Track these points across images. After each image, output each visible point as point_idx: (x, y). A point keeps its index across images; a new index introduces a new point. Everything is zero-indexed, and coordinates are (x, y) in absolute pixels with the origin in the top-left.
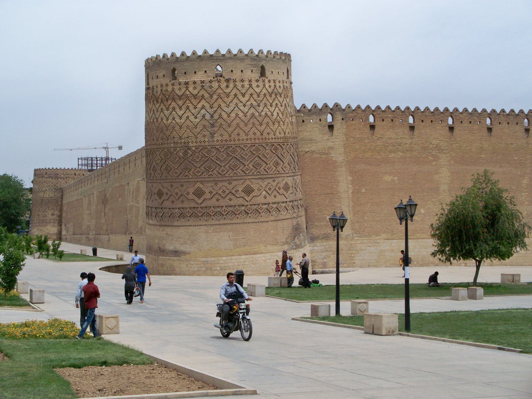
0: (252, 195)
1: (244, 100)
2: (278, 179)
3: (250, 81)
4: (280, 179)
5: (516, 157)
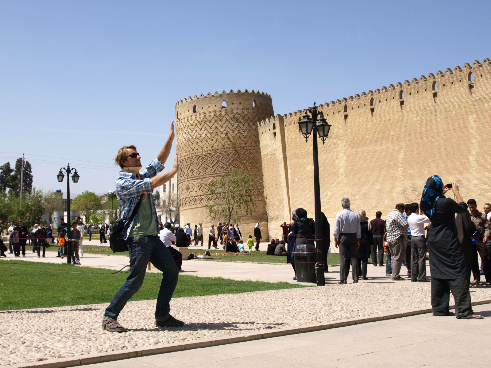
0: (189, 191)
1: (185, 130)
2: (205, 179)
3: (188, 117)
4: (207, 178)
5: (393, 132)
